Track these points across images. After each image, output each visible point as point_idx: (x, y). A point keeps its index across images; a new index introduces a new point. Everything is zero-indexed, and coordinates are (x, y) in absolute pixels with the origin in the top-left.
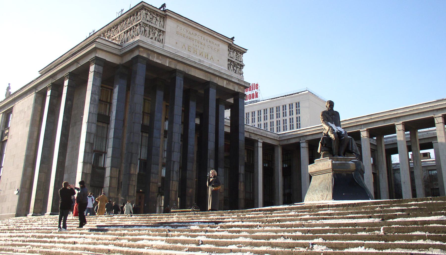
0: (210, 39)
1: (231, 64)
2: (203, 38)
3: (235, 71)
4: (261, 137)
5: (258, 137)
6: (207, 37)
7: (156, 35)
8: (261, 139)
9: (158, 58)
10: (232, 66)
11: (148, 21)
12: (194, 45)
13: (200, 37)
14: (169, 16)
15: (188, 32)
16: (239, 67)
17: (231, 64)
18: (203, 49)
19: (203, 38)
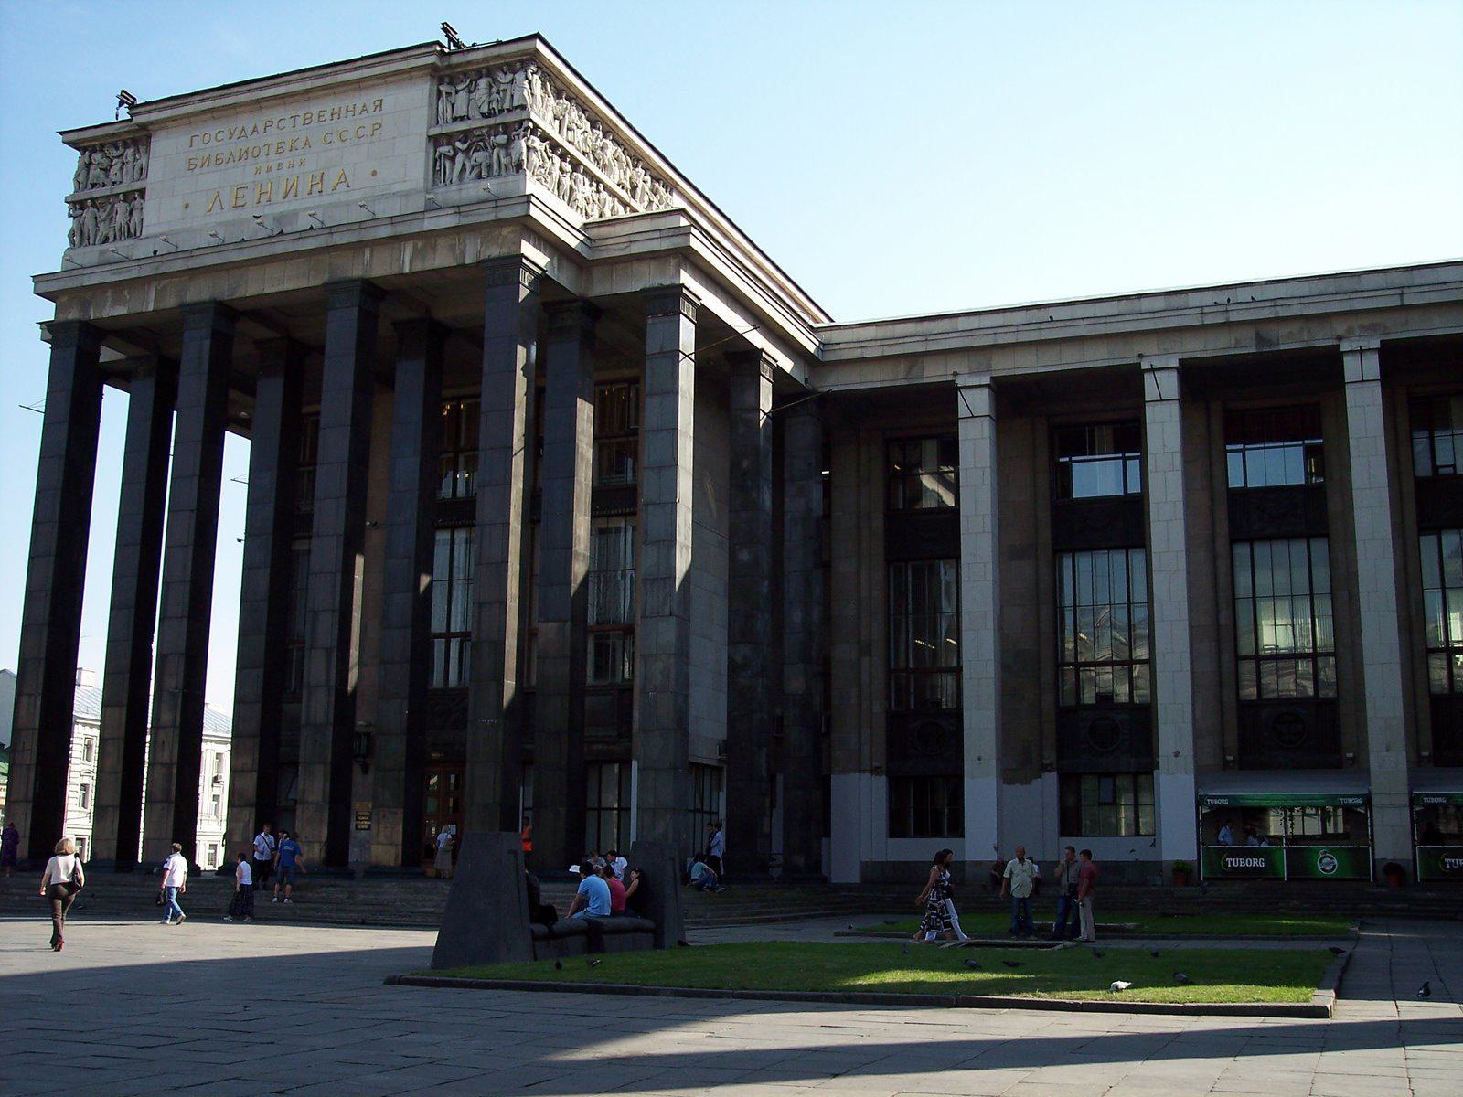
0: (330, 104)
1: (456, 151)
2: (300, 120)
3: (475, 172)
4: (1366, 321)
5: (1340, 327)
6: (314, 108)
7: (120, 219)
8: (1371, 329)
9: (115, 303)
10: (460, 158)
11: (94, 185)
12: (258, 171)
13: (288, 123)
14: (151, 123)
15: (237, 134)
16: (502, 139)
17: (456, 151)
18: (302, 164)
19: (300, 120)
